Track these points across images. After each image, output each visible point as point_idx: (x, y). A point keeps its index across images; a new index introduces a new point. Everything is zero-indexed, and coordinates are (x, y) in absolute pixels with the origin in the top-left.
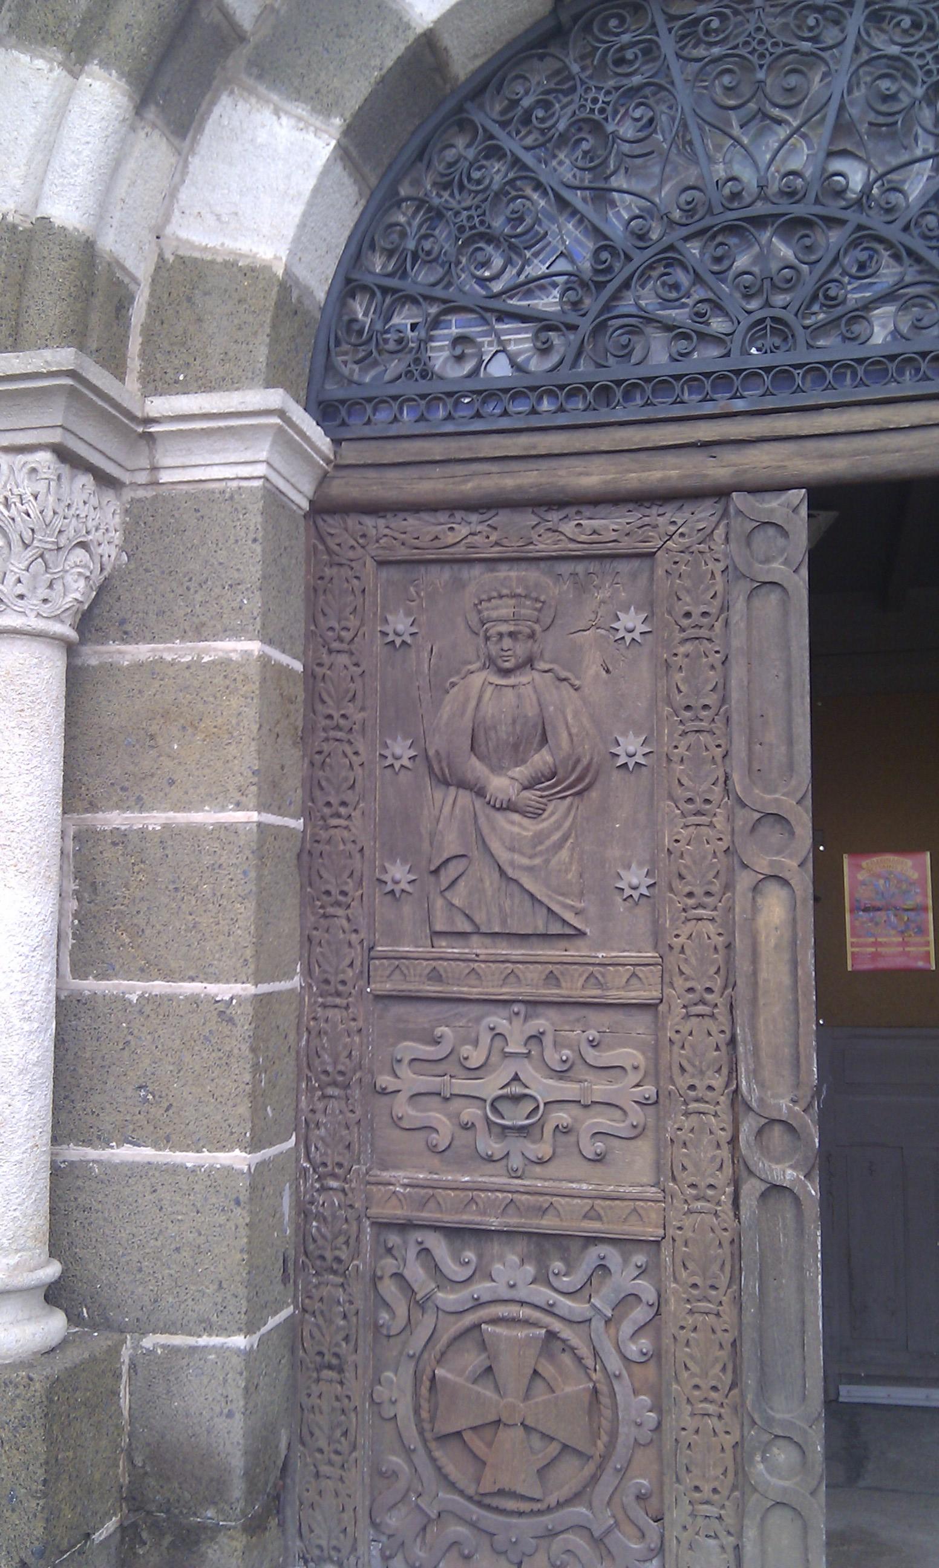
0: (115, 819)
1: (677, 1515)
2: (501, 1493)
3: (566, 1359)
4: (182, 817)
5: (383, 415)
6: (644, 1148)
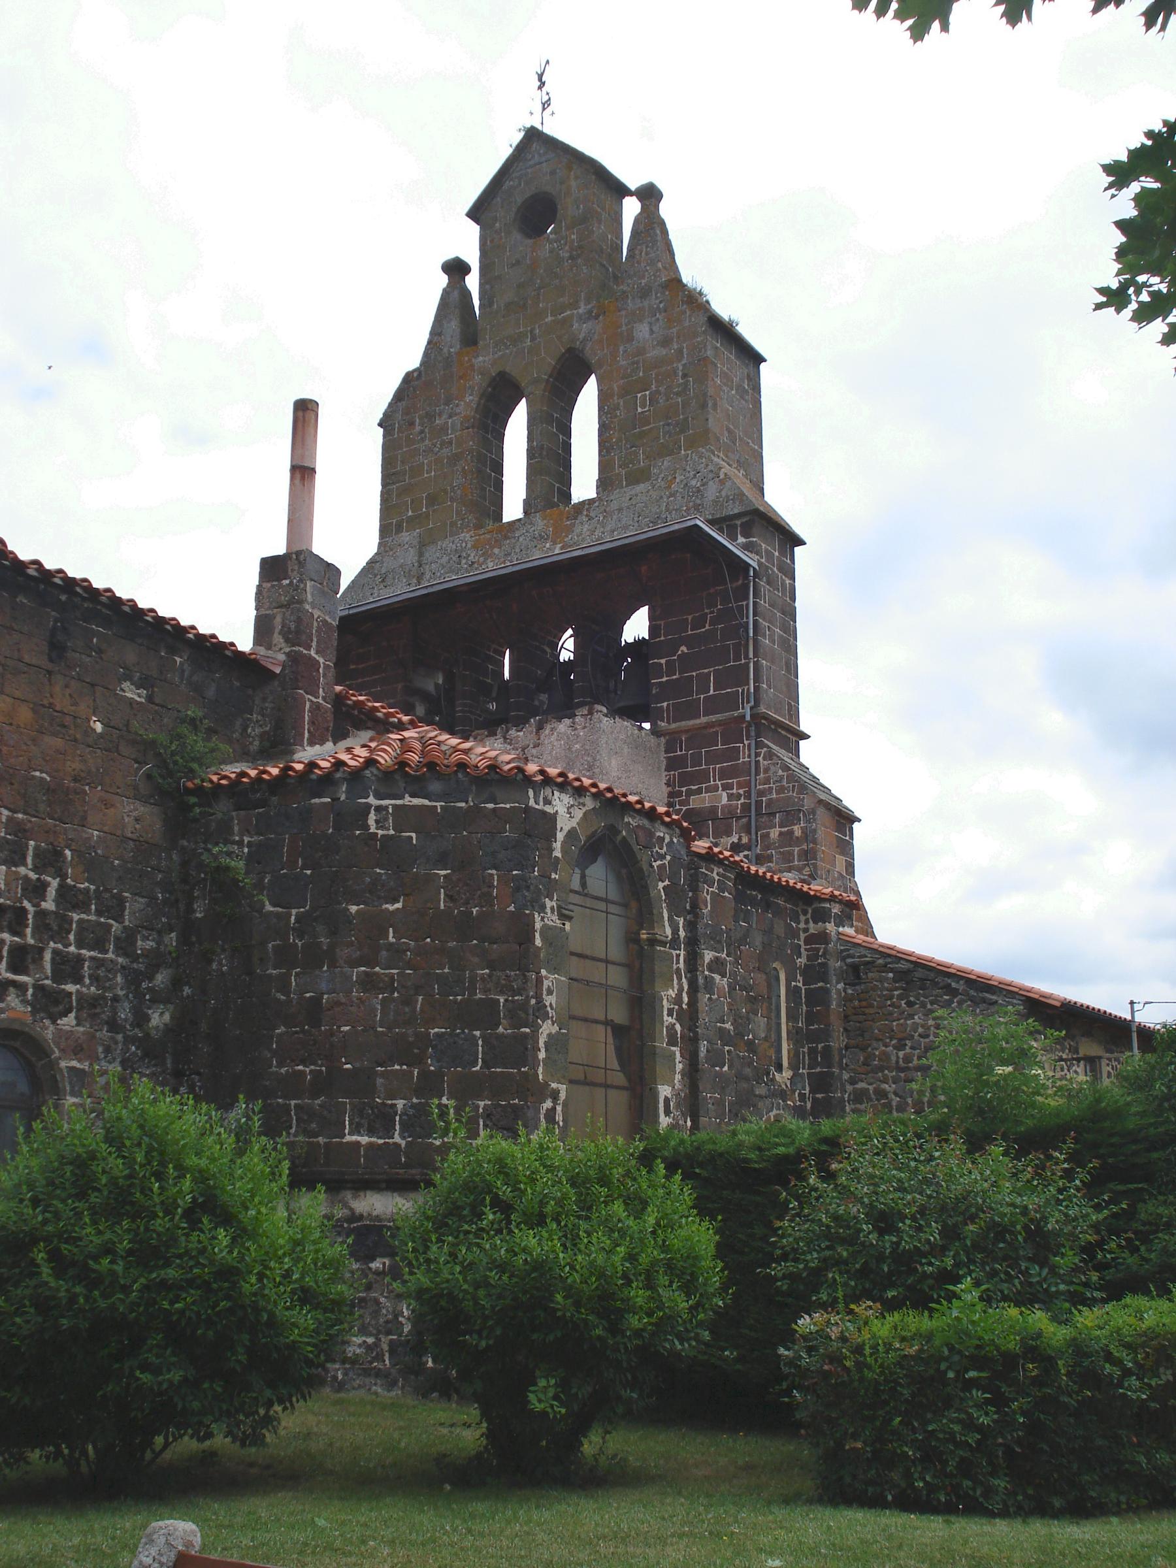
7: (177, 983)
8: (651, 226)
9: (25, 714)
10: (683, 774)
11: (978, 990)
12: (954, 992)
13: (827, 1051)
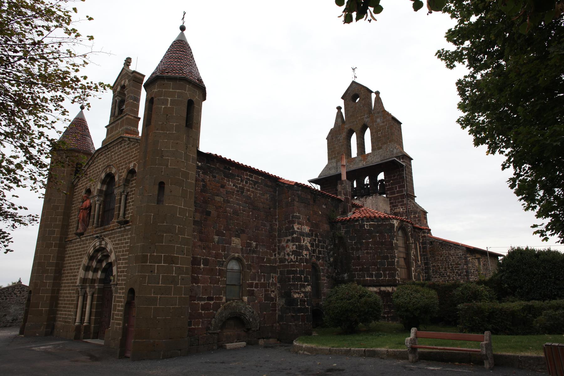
7: (334, 254)
8: (378, 99)
9: (311, 212)
10: (393, 205)
11: (456, 246)
12: (451, 246)
13: (427, 258)
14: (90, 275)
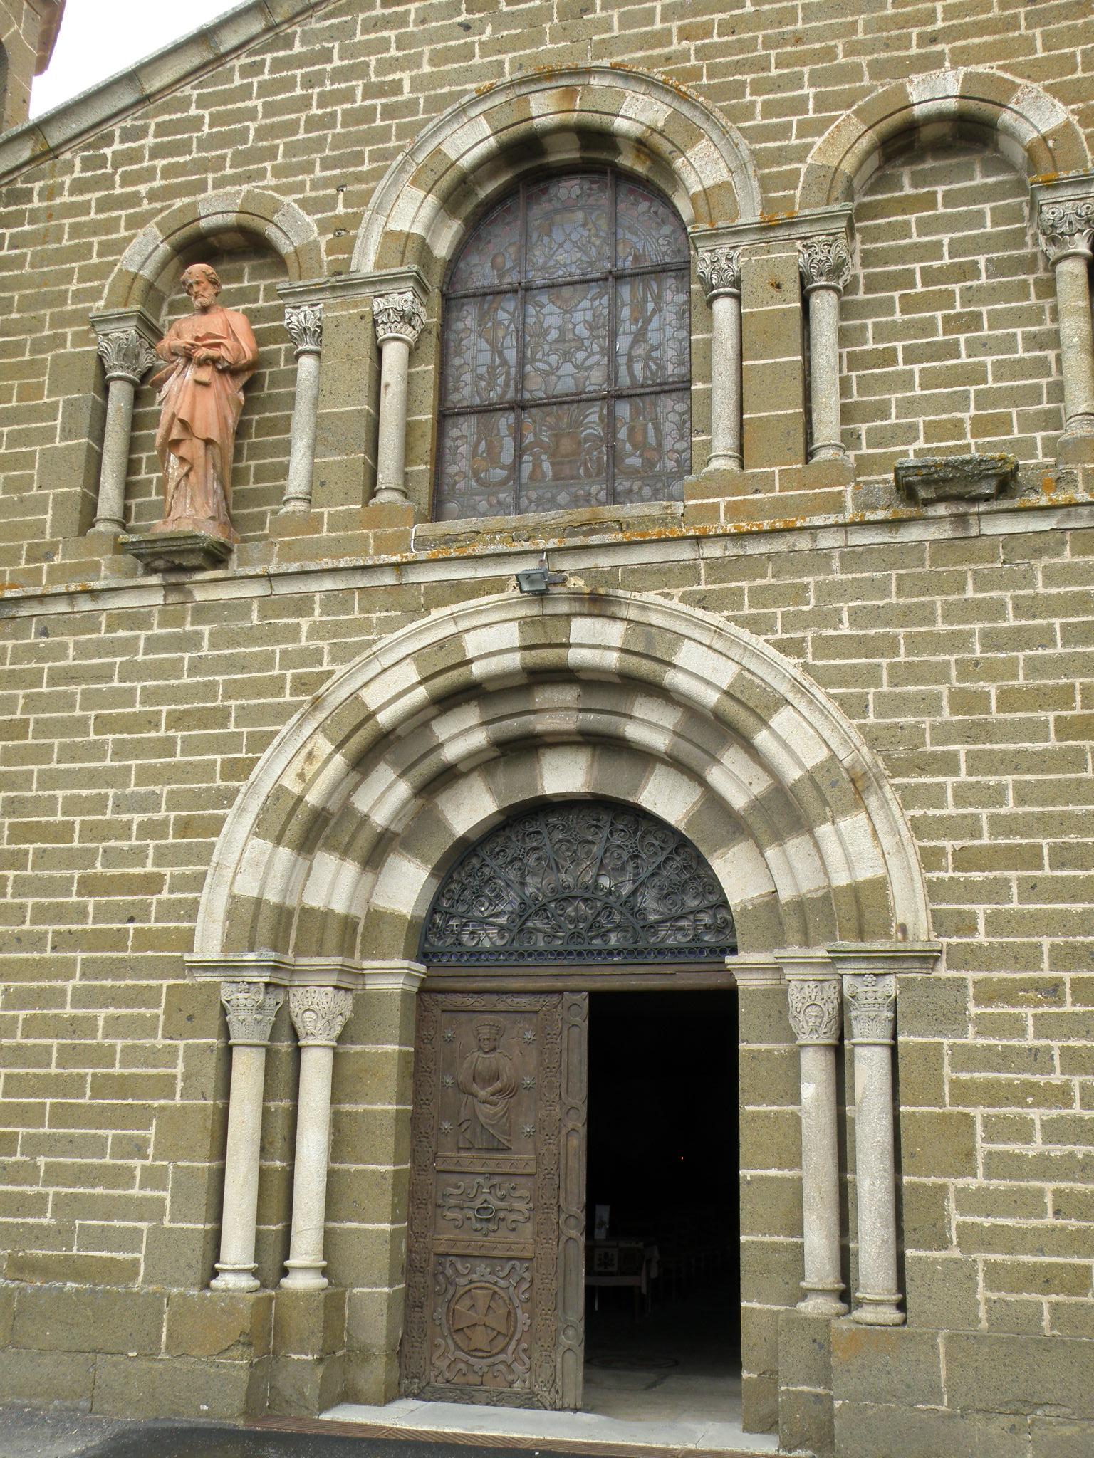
0: (347, 1107)
1: (536, 1356)
2: (476, 1350)
3: (500, 1302)
4: (370, 1107)
5: (444, 960)
6: (529, 1225)
14: (333, 884)
